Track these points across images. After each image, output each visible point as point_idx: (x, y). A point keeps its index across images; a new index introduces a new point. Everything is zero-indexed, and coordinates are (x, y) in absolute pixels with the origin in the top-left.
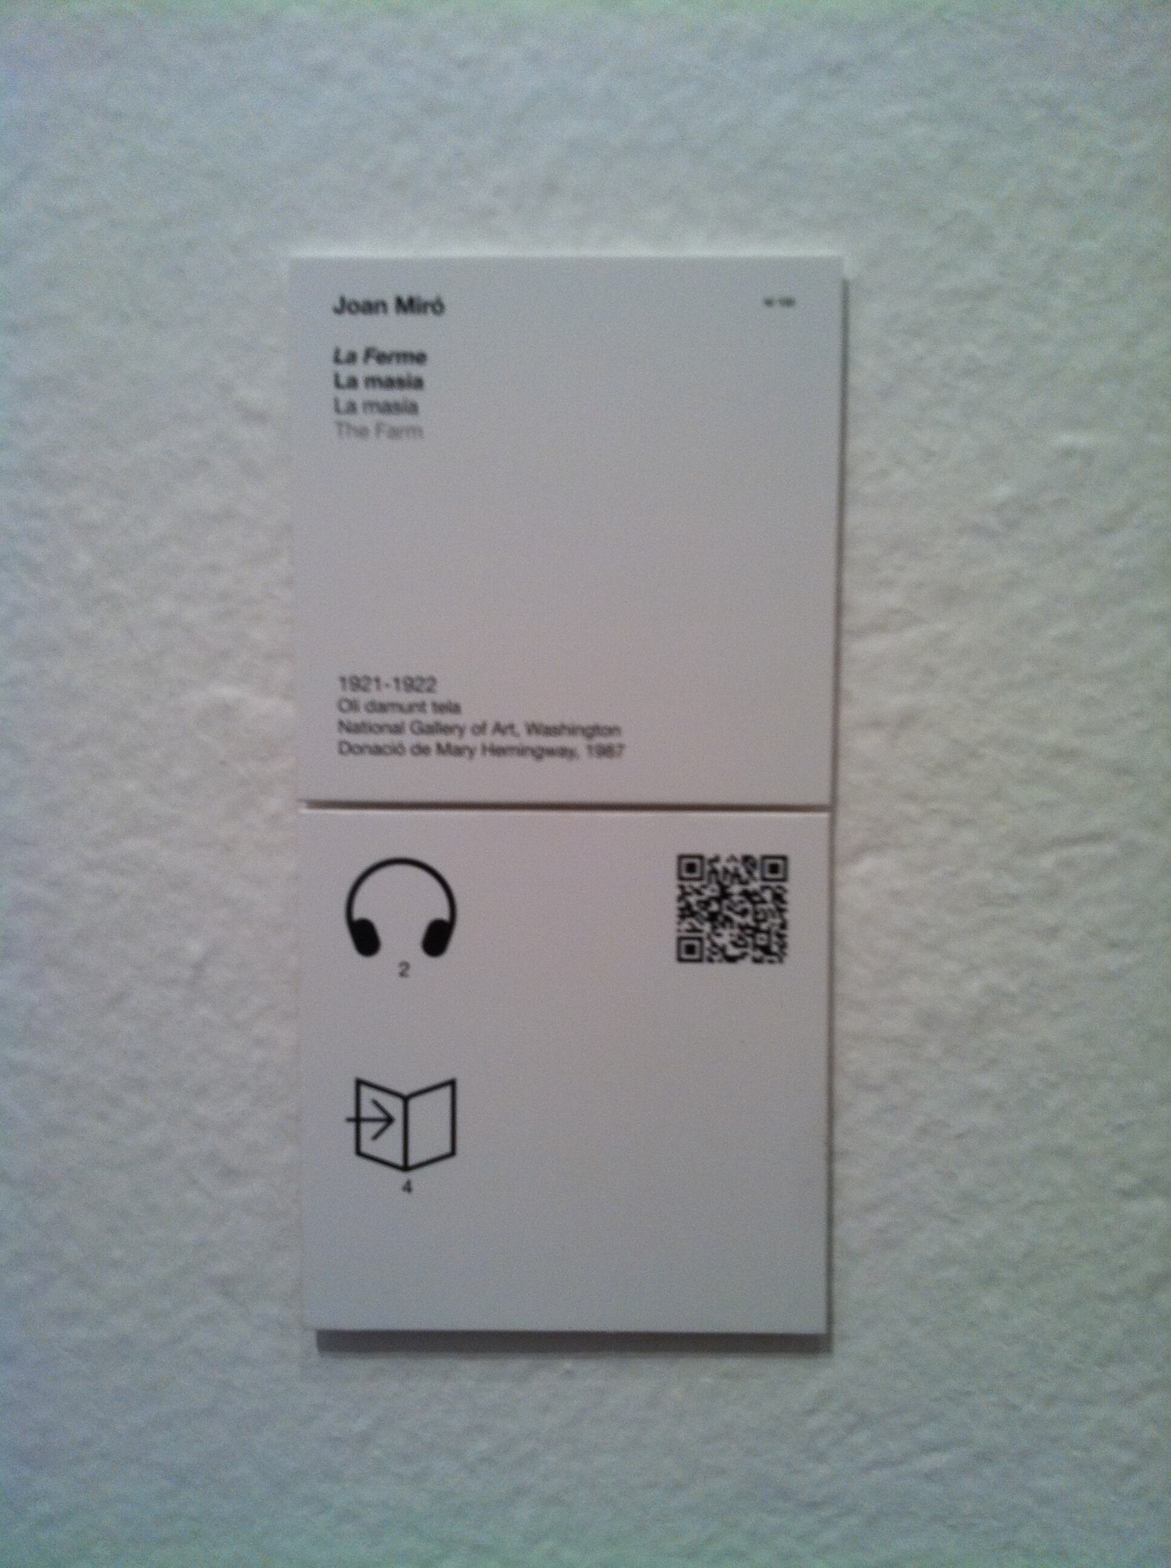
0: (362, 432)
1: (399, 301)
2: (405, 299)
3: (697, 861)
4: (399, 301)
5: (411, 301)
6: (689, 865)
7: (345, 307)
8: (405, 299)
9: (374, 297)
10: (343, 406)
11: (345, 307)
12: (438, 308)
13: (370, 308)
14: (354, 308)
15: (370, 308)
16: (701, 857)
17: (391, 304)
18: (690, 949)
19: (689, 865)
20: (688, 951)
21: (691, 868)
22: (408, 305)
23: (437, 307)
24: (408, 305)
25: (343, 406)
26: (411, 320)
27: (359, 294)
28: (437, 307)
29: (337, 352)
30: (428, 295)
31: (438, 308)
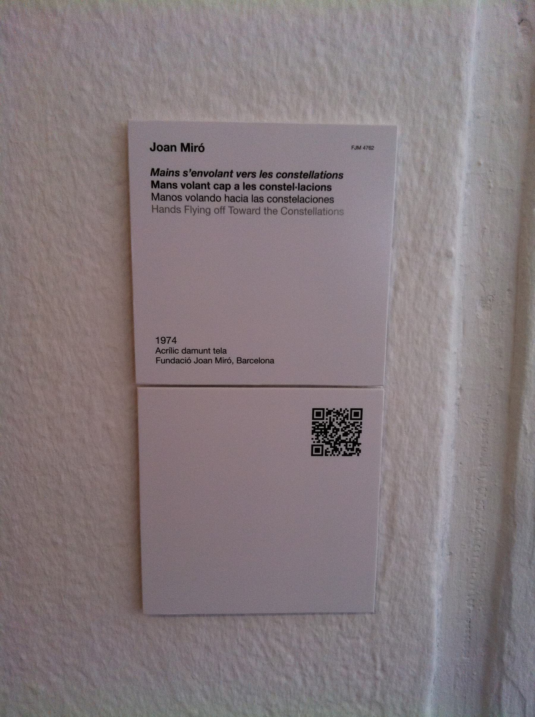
1: (182, 145)
2: (185, 145)
4: (182, 145)
5: (188, 145)
6: (317, 413)
7: (155, 148)
8: (185, 145)
11: (155, 148)
12: (201, 149)
13: (168, 148)
14: (160, 148)
15: (168, 148)
17: (179, 147)
18: (317, 450)
19: (317, 413)
20: (316, 451)
21: (318, 414)
22: (186, 147)
23: (201, 148)
24: (186, 147)
28: (201, 148)
29: (153, 170)
31: (201, 149)
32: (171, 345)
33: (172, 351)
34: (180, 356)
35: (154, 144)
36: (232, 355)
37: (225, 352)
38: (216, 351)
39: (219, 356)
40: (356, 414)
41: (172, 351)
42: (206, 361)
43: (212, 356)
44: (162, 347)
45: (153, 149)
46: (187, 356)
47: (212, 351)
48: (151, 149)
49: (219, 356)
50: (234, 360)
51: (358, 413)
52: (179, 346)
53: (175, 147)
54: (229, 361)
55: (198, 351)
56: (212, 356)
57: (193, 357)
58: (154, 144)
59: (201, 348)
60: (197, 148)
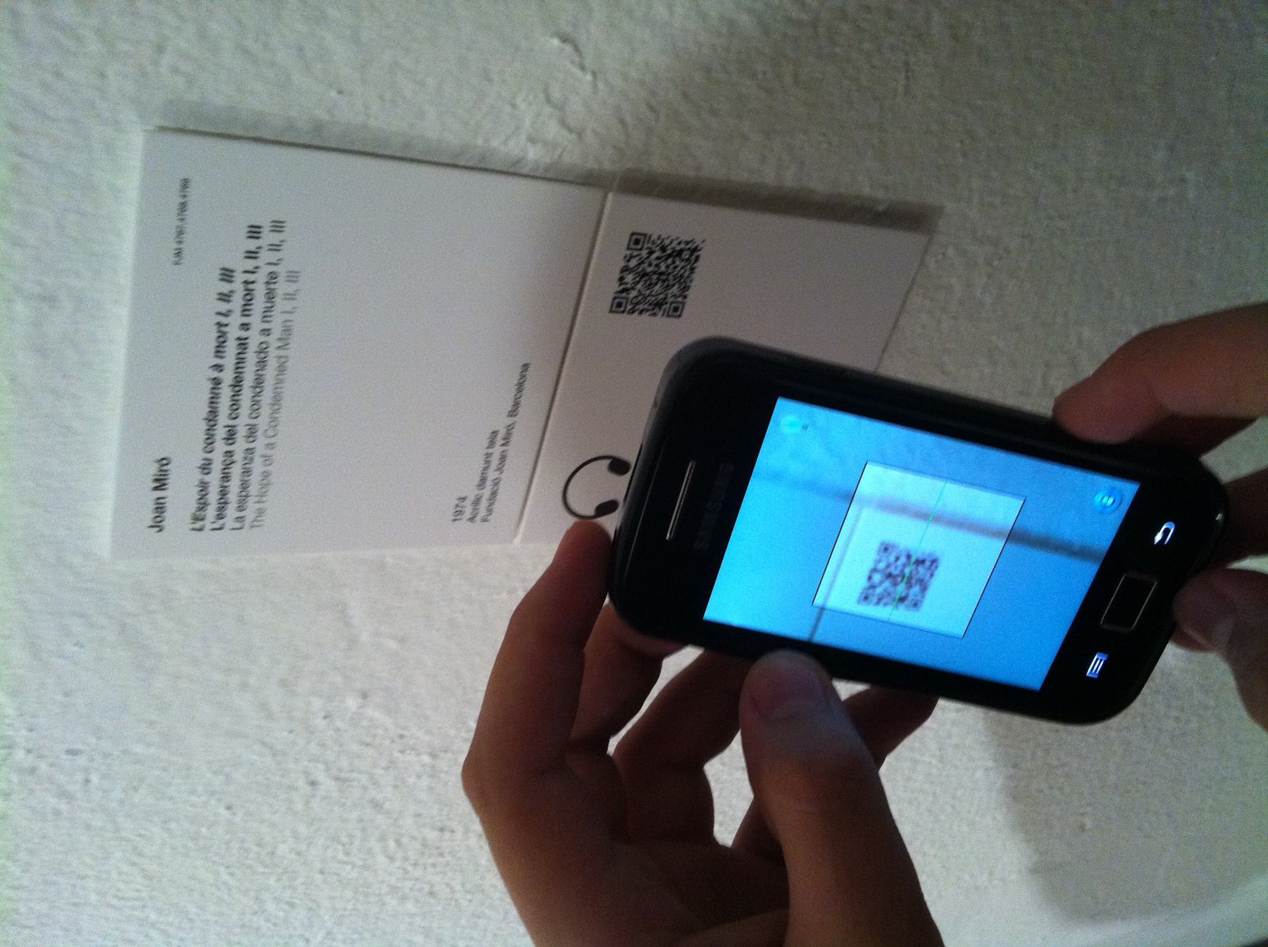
0: (260, 512)
3: (617, 301)
4: (156, 488)
6: (618, 306)
8: (157, 484)
9: (152, 506)
10: (238, 525)
11: (158, 525)
12: (164, 462)
13: (160, 508)
15: (160, 508)
16: (615, 298)
19: (618, 306)
21: (619, 305)
22: (160, 482)
23: (164, 462)
24: (160, 482)
25: (238, 525)
26: (172, 481)
27: (149, 515)
28: (164, 462)
30: (153, 469)
31: (164, 462)
32: (468, 503)
33: (477, 502)
34: (486, 492)
35: (152, 527)
36: (501, 424)
37: (495, 433)
38: (492, 443)
39: (499, 441)
40: (637, 242)
41: (477, 502)
42: (503, 458)
43: (497, 450)
44: (468, 515)
45: (157, 529)
46: (489, 484)
47: (490, 451)
48: (160, 531)
49: (499, 441)
50: (510, 420)
51: (637, 240)
52: (472, 494)
53: (158, 499)
54: (510, 428)
55: (485, 469)
56: (497, 450)
57: (492, 475)
58: (152, 527)
59: (481, 465)
60: (165, 468)
